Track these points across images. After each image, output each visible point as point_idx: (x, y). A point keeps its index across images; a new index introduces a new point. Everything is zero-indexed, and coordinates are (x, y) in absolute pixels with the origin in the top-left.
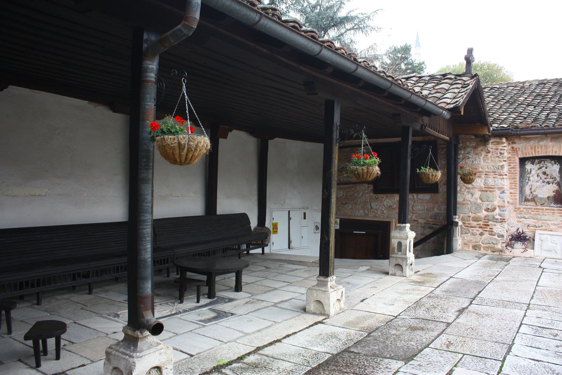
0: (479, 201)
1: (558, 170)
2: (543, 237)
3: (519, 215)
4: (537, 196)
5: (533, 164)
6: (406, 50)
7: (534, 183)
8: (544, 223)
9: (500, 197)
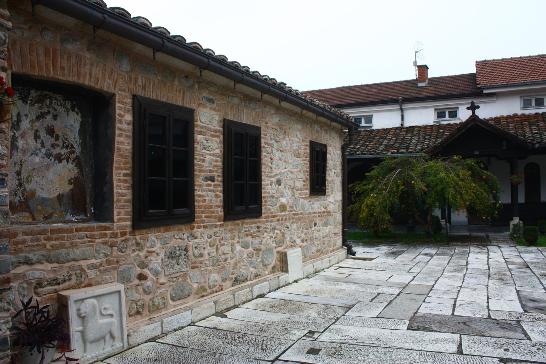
1: (77, 126)
2: (85, 308)
4: (33, 194)
5: (25, 101)
8: (71, 268)
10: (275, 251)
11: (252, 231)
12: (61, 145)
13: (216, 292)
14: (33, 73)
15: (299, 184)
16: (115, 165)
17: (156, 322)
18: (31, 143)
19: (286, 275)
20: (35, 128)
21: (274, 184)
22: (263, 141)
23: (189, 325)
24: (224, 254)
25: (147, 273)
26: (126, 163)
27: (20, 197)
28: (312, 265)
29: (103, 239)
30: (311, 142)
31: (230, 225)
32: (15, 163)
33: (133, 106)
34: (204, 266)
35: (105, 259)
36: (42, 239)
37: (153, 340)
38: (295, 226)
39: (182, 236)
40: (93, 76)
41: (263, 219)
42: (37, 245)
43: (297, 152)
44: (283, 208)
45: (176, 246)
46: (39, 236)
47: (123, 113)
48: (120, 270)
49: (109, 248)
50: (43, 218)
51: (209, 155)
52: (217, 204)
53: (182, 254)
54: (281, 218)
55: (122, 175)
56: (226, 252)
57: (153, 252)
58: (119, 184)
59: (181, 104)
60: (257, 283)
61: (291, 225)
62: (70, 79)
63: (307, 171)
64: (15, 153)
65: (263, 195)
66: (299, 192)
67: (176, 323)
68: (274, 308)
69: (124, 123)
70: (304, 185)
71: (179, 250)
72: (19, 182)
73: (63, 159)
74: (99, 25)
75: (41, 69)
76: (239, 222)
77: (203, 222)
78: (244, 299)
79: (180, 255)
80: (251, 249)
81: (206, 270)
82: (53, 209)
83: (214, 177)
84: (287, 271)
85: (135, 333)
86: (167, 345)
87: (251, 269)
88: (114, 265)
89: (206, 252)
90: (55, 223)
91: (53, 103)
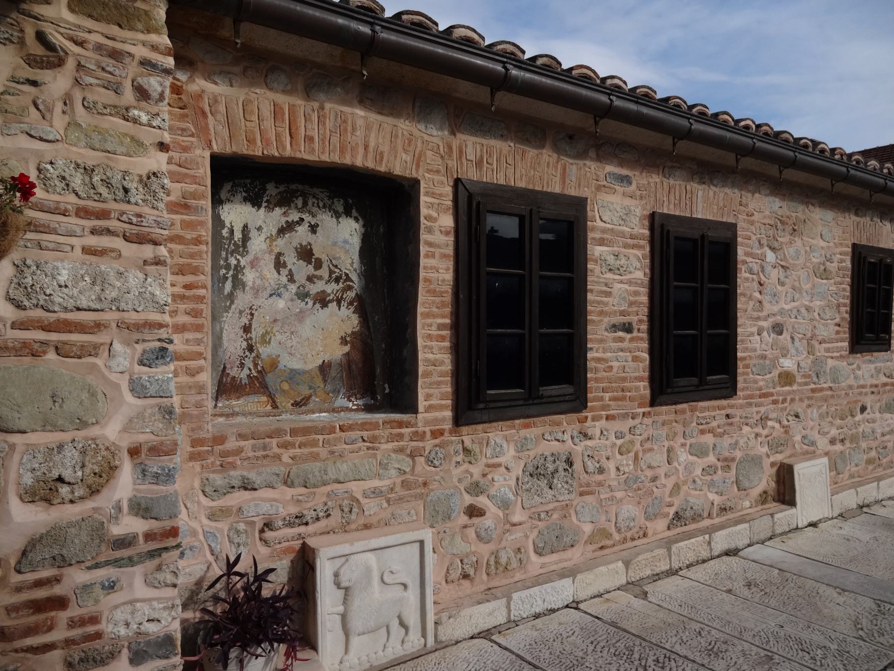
1: (356, 242)
3: (218, 479)
4: (274, 364)
7: (262, 301)
9: (138, 389)
10: (766, 462)
11: (714, 424)
12: (326, 276)
13: (633, 539)
14: (252, 153)
15: (827, 330)
16: (420, 309)
17: (496, 598)
18: (268, 276)
19: (792, 511)
20: (277, 250)
21: (765, 334)
22: (740, 251)
23: (567, 606)
24: (650, 467)
25: (486, 506)
26: (443, 305)
27: (250, 369)
28: (853, 490)
29: (396, 443)
30: (854, 246)
31: (665, 412)
32: (241, 312)
33: (456, 200)
34: (608, 490)
35: (399, 481)
36: (274, 446)
37: (486, 634)
38: (814, 413)
39: (560, 436)
40: (371, 149)
41: (741, 401)
42: (265, 457)
43: (822, 268)
44: (787, 378)
45: (547, 453)
46: (268, 440)
47: (435, 214)
48: (429, 498)
49: (408, 459)
50: (292, 405)
51: (621, 282)
52: (637, 374)
53: (561, 469)
54: (781, 398)
55: (434, 328)
56: (654, 464)
57: (500, 465)
58: (429, 343)
59: (557, 190)
60: (722, 527)
61: (805, 412)
62: (325, 158)
64: (239, 293)
65: (738, 354)
66: (824, 345)
67: (540, 602)
68: (754, 589)
69: (437, 233)
70: (838, 332)
71: (554, 461)
72: (248, 344)
73: (331, 301)
74: (369, 48)
75: (266, 142)
77: (604, 408)
78: (691, 557)
79: (556, 471)
81: (612, 499)
82: (310, 388)
83: (630, 324)
84: (792, 503)
85: (451, 620)
86: (508, 653)
87: (712, 496)
88: (418, 491)
89: (611, 466)
90: (314, 413)
91: (310, 203)
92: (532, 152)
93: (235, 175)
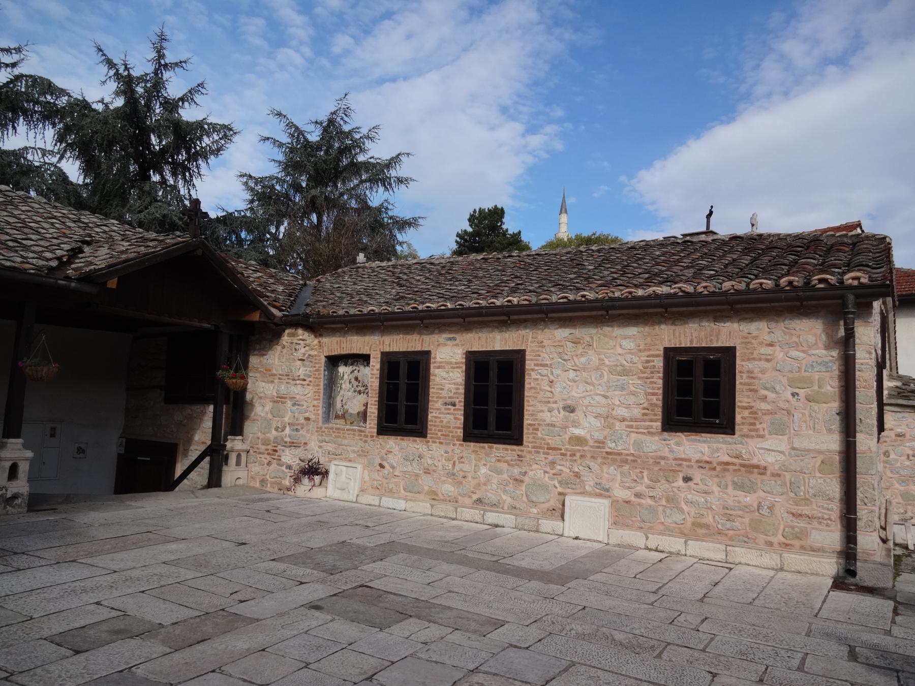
0: (270, 416)
6: (497, 214)
7: (346, 393)
44: (579, 441)
54: (569, 453)
59: (419, 349)
63: (653, 394)
70: (644, 414)
76: (486, 445)
77: (439, 438)
80: (505, 476)
92: (408, 337)
93: (334, 361)
